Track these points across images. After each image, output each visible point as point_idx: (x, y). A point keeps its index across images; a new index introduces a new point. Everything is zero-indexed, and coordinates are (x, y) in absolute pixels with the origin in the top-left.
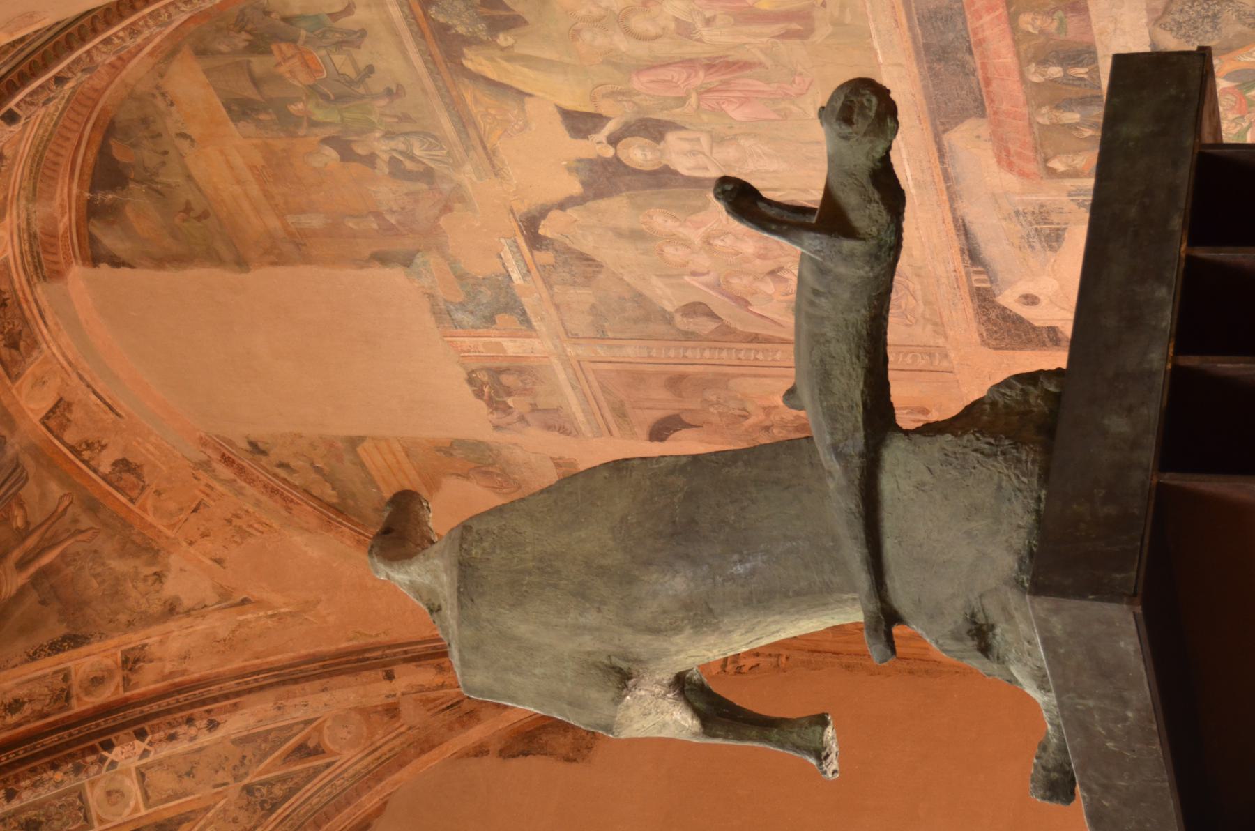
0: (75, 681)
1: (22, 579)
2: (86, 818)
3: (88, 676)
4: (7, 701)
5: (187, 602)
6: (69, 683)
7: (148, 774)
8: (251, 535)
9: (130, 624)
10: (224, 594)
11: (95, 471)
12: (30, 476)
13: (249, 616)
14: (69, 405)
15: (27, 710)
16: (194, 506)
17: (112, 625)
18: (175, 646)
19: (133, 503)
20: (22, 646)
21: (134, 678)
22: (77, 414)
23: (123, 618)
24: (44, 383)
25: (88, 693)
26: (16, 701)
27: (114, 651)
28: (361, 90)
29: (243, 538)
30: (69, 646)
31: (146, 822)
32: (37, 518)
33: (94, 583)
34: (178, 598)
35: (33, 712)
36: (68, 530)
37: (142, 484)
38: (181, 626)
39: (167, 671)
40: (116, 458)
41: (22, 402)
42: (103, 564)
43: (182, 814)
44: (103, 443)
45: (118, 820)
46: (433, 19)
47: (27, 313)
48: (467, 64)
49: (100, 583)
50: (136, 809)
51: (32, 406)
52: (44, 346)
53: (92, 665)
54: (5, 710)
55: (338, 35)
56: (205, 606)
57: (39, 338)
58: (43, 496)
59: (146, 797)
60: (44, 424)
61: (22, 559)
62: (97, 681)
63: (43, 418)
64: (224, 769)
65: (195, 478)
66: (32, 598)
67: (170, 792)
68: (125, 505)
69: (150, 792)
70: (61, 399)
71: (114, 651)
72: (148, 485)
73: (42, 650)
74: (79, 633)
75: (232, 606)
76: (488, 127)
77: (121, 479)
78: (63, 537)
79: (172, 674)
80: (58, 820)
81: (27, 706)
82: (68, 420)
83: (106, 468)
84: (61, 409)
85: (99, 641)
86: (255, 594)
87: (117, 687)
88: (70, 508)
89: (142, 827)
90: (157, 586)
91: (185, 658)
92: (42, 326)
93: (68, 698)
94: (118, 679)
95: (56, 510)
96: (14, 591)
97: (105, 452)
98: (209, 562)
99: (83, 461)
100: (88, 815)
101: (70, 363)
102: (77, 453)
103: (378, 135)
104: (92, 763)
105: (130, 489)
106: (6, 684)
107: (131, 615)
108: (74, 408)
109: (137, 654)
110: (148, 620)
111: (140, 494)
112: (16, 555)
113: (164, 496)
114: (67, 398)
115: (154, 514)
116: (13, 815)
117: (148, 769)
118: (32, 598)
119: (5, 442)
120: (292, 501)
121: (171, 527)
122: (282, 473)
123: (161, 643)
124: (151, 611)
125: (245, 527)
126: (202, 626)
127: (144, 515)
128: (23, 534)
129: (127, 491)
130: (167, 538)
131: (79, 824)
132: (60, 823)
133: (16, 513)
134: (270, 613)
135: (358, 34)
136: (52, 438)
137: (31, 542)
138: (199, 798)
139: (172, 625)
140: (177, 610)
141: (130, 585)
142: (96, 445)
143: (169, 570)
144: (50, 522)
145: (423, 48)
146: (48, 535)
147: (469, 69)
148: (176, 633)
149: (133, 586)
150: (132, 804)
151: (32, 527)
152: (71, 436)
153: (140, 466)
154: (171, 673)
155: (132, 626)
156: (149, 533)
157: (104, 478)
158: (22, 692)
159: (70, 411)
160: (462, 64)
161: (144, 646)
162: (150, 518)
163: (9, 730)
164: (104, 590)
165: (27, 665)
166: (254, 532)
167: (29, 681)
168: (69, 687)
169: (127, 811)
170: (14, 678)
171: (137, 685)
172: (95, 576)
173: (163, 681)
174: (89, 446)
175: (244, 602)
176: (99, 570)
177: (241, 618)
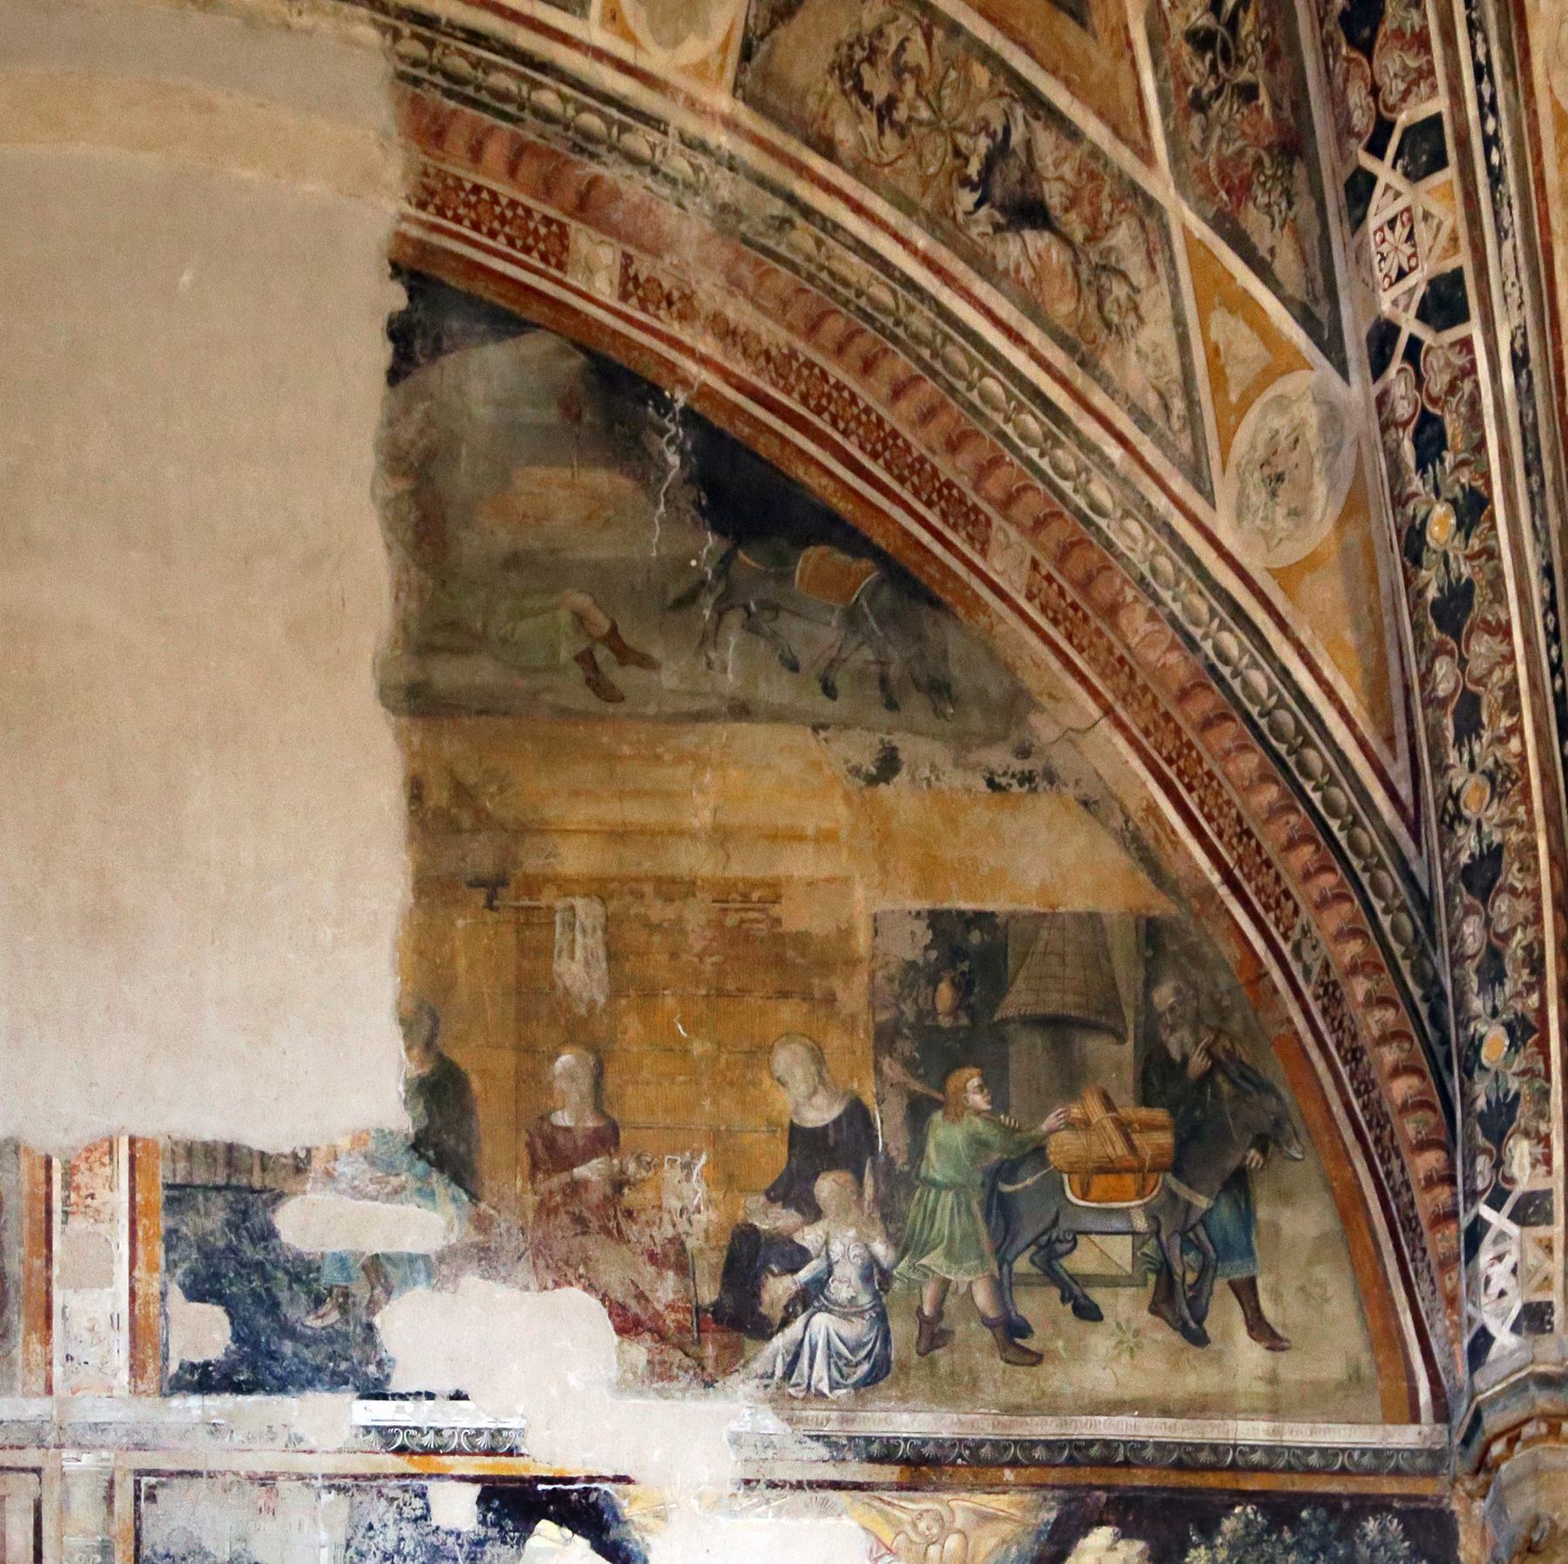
28: (1022, 1265)
46: (1233, 1506)
48: (1101, 1536)
55: (1191, 1278)
76: (904, 1517)
103: (880, 1249)
135: (1192, 1324)
145: (1149, 1453)
147: (1085, 1535)
160: (1101, 1523)
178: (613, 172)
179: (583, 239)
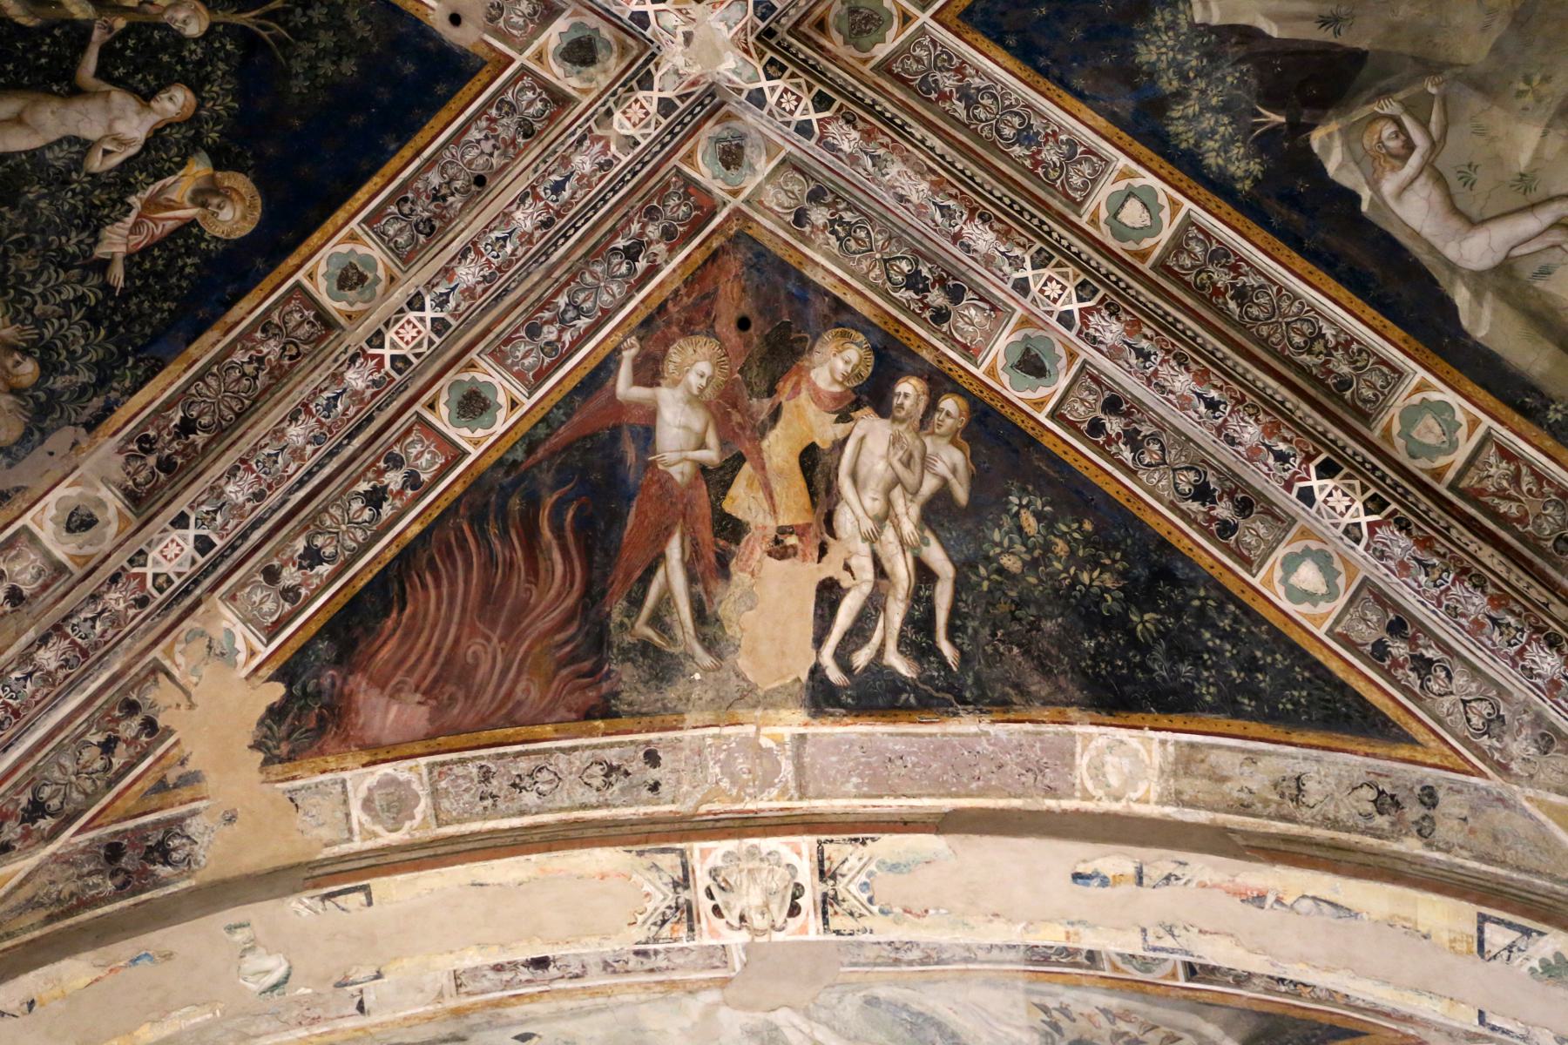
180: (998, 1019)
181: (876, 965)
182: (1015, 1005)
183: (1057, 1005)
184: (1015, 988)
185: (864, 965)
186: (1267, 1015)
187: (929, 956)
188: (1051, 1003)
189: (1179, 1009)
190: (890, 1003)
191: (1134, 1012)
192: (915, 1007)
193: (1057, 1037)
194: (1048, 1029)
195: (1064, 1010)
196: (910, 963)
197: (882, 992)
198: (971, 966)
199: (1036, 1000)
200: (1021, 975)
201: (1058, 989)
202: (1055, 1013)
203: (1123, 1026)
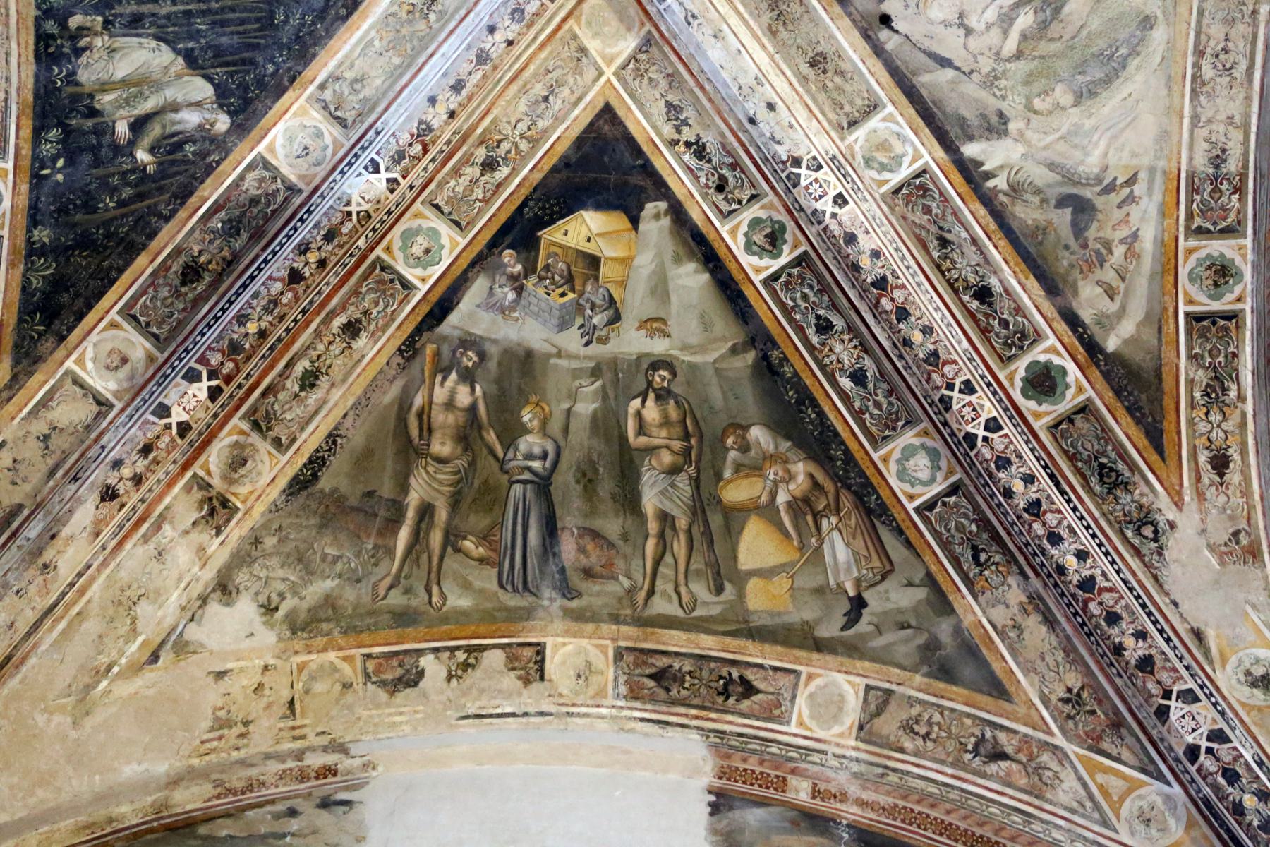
0: (263, 447)
1: (413, 499)
2: (134, 318)
3: (254, 460)
4: (324, 379)
5: (214, 608)
6: (269, 440)
7: (95, 409)
8: (212, 729)
9: (257, 542)
10: (183, 648)
11: (436, 650)
12: (501, 592)
13: (134, 648)
14: (527, 681)
15: (292, 385)
16: (297, 706)
17: (275, 526)
18: (182, 555)
19: (364, 655)
20: (356, 437)
21: (197, 495)
22: (510, 681)
23: (270, 542)
24: (579, 676)
25: (236, 445)
26: (312, 386)
27: (249, 504)
29: (217, 719)
30: (303, 474)
31: (60, 352)
32: (451, 562)
33: (332, 551)
34: (227, 604)
35: (284, 388)
36: (406, 578)
37: (374, 679)
38: (197, 580)
39: (167, 527)
40: (425, 680)
41: (584, 642)
42: (340, 576)
43: (20, 389)
44: (454, 681)
45: (94, 337)
47: (682, 710)
49: (324, 557)
50: (80, 362)
51: (569, 648)
52: (621, 703)
53: (259, 474)
54: (318, 369)
56: (192, 620)
57: (638, 705)
58: (466, 586)
59: (77, 382)
60: (538, 644)
61: (432, 516)
62: (238, 462)
63: (544, 648)
64: (9, 470)
65: (323, 733)
66: (387, 489)
67: (54, 404)
68: (371, 646)
69: (78, 389)
70: (542, 678)
71: (249, 504)
72: (365, 684)
73: (330, 450)
74: (304, 493)
75: (163, 643)
77: (400, 666)
78: (406, 569)
79: (158, 527)
80: (165, 299)
81: (297, 388)
82: (513, 669)
83: (427, 662)
84: (532, 672)
85: (275, 501)
86: (150, 675)
87: (209, 473)
88: (426, 597)
89: (58, 345)
90: (262, 599)
91: (160, 554)
92: (646, 715)
93: (256, 426)
94: (216, 482)
95: (438, 584)
96: (412, 481)
97: (444, 674)
98: (230, 666)
99: (458, 648)
100: (134, 323)
101: (569, 714)
102: (469, 650)
104: (222, 363)
105: (381, 664)
106: (340, 393)
107: (263, 550)
108: (520, 684)
109: (219, 519)
110: (241, 559)
111: (365, 669)
112: (442, 515)
113: (338, 687)
114: (536, 686)
115: (332, 663)
116: (220, 274)
117: (99, 413)
118: (387, 489)
119: (564, 596)
120: (218, 797)
121: (301, 667)
122: (280, 807)
123: (202, 549)
124: (245, 570)
125: (226, 732)
126: (175, 599)
127: (341, 654)
128: (452, 538)
129: (381, 660)
130: (296, 653)
131: (138, 307)
132: (161, 295)
133: (481, 549)
134: (116, 669)
136: (514, 640)
137: (436, 538)
138: (13, 418)
139: (209, 574)
140: (218, 593)
141: (292, 578)
142: (460, 672)
143: (264, 623)
144: (435, 569)
146: (424, 557)
148: (196, 569)
149: (288, 579)
150: (90, 365)
151: (449, 549)
152: (495, 659)
153: (392, 693)
154: (160, 528)
155: (252, 540)
156: (320, 641)
157: (420, 652)
158: (313, 398)
159: (519, 678)
161: (218, 533)
162: (332, 656)
163: (296, 354)
164: (315, 553)
165: (332, 427)
166: (211, 735)
167: (316, 412)
168: (265, 437)
169: (90, 353)
170: (336, 404)
171: (188, 489)
172: (337, 559)
173: (160, 515)
174: (466, 666)
175: (154, 657)
176: (339, 567)
177: (140, 639)
178: (803, 765)
179: (793, 781)
180: (1115, 137)
181: (1198, 34)
182: (1134, 155)
183: (1136, 193)
184: (1157, 158)
185: (1199, 22)
186: (1159, 377)
187: (1203, 84)
188: (1138, 189)
189: (1149, 300)
190: (1142, 40)
191: (1139, 264)
192: (1133, 63)
193: (1098, 189)
194: (1106, 182)
195: (1131, 199)
196: (1197, 66)
197: (1159, 35)
198: (1186, 121)
199: (1142, 175)
200: (1174, 165)
201: (1158, 197)
202: (1126, 191)
203: (1119, 251)
